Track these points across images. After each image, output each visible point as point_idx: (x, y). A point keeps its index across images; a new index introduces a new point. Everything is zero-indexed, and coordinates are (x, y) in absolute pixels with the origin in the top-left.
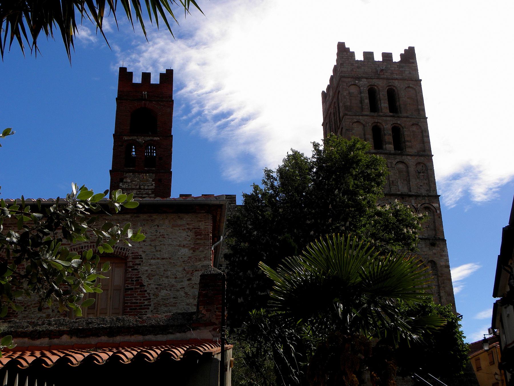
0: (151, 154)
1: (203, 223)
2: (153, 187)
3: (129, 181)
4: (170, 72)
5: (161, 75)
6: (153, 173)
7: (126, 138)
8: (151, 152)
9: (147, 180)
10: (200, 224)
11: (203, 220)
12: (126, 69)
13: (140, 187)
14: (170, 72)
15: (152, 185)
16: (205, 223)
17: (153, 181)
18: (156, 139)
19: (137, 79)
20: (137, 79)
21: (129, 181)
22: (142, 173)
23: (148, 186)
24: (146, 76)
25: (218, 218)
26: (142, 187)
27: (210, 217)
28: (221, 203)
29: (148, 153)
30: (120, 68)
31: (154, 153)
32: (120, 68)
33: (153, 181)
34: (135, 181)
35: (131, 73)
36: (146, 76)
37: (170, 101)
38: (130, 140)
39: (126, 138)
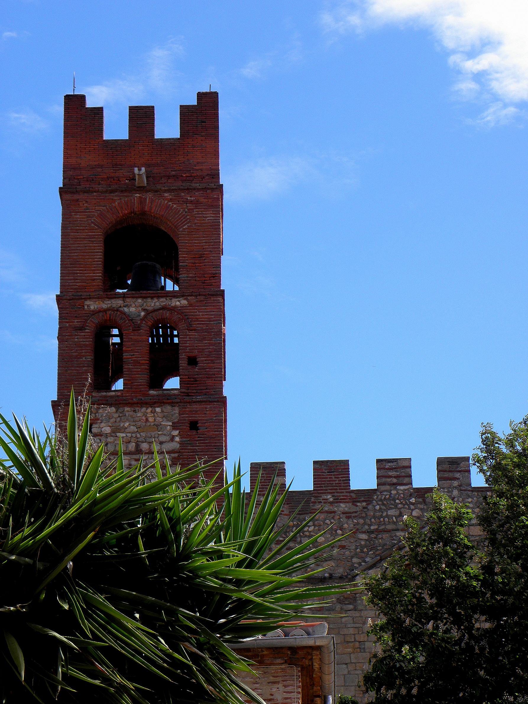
0: (165, 340)
1: (280, 686)
2: (175, 446)
3: (107, 430)
4: (208, 103)
5: (185, 111)
6: (172, 404)
7: (93, 305)
8: (165, 335)
9: (158, 426)
10: (274, 690)
11: (280, 679)
12: (82, 98)
13: (137, 446)
14: (208, 103)
15: (172, 439)
16: (285, 686)
17: (174, 427)
18: (176, 303)
19: (116, 128)
20: (116, 128)
21: (107, 430)
22: (142, 404)
23: (161, 443)
24: (142, 117)
25: (316, 666)
26: (144, 446)
27: (295, 671)
28: (318, 644)
29: (158, 336)
30: (68, 98)
31: (172, 336)
32: (67, 97)
33: (174, 427)
34: (123, 430)
35: (98, 112)
36: (142, 117)
37: (213, 189)
38: (105, 311)
39: (93, 305)
